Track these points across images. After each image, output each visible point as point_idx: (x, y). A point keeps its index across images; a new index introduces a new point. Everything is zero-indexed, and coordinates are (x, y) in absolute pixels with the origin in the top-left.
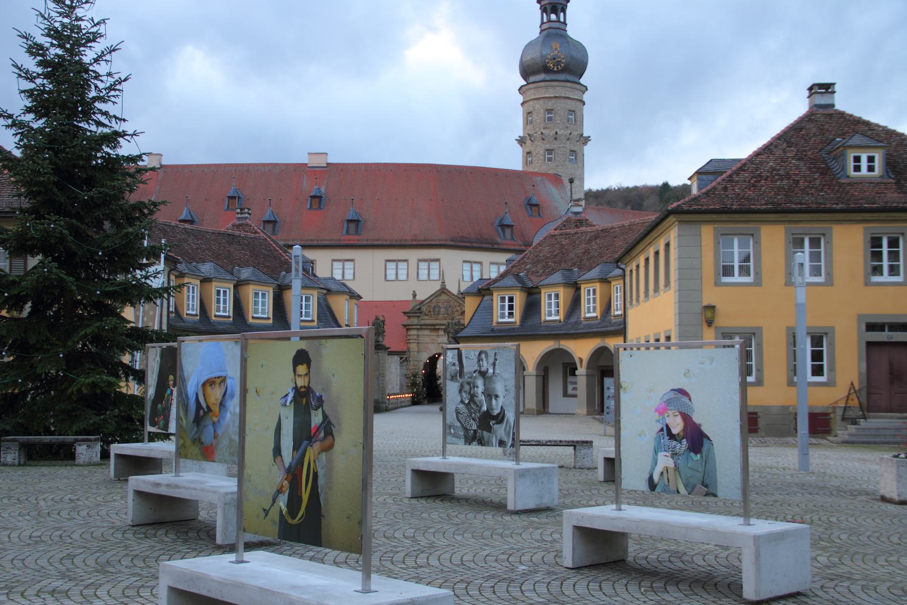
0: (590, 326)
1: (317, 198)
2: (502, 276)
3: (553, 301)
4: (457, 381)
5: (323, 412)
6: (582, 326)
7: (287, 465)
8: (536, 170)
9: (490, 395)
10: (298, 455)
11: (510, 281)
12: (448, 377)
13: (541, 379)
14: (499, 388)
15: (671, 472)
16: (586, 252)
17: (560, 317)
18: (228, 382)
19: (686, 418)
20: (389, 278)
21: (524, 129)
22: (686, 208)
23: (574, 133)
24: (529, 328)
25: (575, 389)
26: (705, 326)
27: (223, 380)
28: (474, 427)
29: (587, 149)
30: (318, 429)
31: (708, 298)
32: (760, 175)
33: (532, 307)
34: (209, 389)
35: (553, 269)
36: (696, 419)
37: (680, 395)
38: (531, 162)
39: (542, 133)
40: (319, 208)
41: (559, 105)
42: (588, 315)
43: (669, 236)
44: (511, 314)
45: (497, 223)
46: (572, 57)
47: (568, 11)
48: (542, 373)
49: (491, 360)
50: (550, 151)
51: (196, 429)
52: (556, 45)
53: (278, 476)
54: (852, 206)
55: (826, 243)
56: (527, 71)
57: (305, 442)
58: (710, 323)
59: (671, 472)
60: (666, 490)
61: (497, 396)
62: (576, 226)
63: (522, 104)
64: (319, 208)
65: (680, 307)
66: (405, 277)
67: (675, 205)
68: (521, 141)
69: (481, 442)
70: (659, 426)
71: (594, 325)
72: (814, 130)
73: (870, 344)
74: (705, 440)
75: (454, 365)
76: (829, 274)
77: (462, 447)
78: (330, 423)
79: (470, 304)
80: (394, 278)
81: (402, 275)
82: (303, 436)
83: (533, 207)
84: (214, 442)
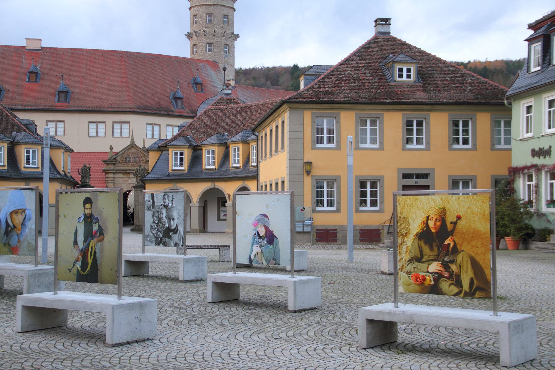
1: (34, 74)
2: (176, 138)
3: (211, 155)
4: (151, 211)
5: (99, 225)
6: (230, 173)
7: (81, 248)
8: (199, 58)
10: (86, 244)
11: (181, 141)
12: (146, 208)
13: (202, 208)
14: (175, 214)
15: (259, 254)
16: (234, 122)
17: (216, 166)
18: (27, 212)
19: (267, 228)
20: (91, 135)
21: (191, 27)
22: (294, 100)
23: (228, 32)
24: (194, 174)
27: (24, 211)
28: (161, 236)
29: (237, 44)
30: (96, 232)
31: (307, 158)
32: (341, 79)
33: (196, 159)
34: (14, 216)
35: (211, 133)
36: (271, 228)
37: (264, 217)
39: (204, 31)
40: (36, 81)
41: (217, 11)
42: (234, 165)
43: (284, 117)
44: (181, 165)
45: (171, 96)
48: (203, 205)
49: (171, 199)
50: (210, 44)
51: (6, 238)
53: (76, 254)
54: (396, 100)
55: (380, 123)
57: (90, 238)
58: (308, 173)
59: (259, 254)
61: (174, 219)
62: (227, 103)
63: (190, 8)
64: (36, 81)
65: (290, 163)
66: (103, 135)
68: (189, 36)
69: (165, 244)
70: (254, 232)
71: (238, 172)
72: (377, 49)
74: (275, 239)
75: (149, 201)
76: (381, 143)
77: (153, 247)
78: (102, 229)
79: (153, 157)
80: (95, 135)
81: (101, 133)
82: (89, 235)
83: (198, 84)
84: (18, 244)
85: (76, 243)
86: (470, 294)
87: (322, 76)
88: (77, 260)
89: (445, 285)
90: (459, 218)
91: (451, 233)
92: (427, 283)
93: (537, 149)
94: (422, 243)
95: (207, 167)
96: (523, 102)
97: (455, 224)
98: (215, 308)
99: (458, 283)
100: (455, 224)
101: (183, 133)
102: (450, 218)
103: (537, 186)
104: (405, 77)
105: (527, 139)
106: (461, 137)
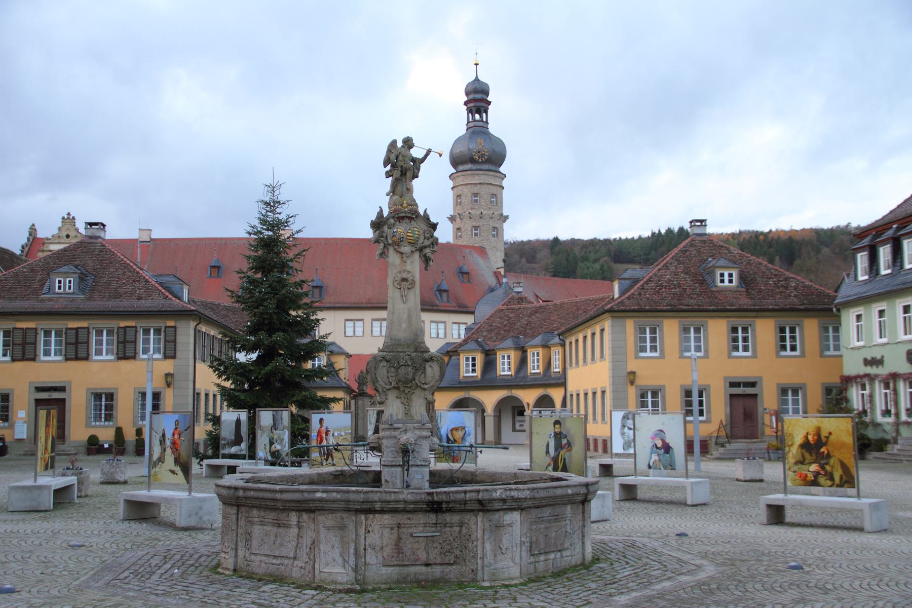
0: (536, 379)
2: (465, 341)
3: (506, 360)
8: (464, 243)
11: (472, 345)
16: (529, 323)
18: (467, 429)
19: (663, 441)
20: (347, 334)
21: (454, 209)
23: (496, 213)
24: (488, 381)
25: (521, 425)
26: (629, 385)
27: (464, 428)
31: (632, 365)
32: (661, 285)
33: (490, 364)
34: (455, 432)
36: (667, 441)
38: (461, 236)
41: (484, 190)
44: (474, 371)
45: (435, 289)
46: (494, 151)
47: (489, 112)
50: (476, 228)
52: (480, 140)
53: (548, 460)
54: (719, 307)
55: (704, 331)
56: (456, 161)
58: (632, 383)
60: (655, 468)
63: (453, 188)
66: (361, 334)
67: (609, 306)
72: (694, 252)
73: (732, 396)
76: (706, 351)
80: (352, 334)
81: (359, 332)
82: (559, 447)
83: (464, 274)
85: (547, 452)
86: (841, 485)
87: (642, 283)
88: (549, 465)
89: (822, 480)
90: (830, 433)
91: (825, 444)
92: (809, 479)
93: (869, 358)
94: (804, 451)
95: (502, 373)
96: (852, 310)
97: (827, 438)
98: (622, 503)
99: (831, 478)
100: (827, 438)
101: (472, 334)
102: (824, 434)
103: (871, 396)
104: (726, 283)
105: (859, 348)
106: (788, 343)
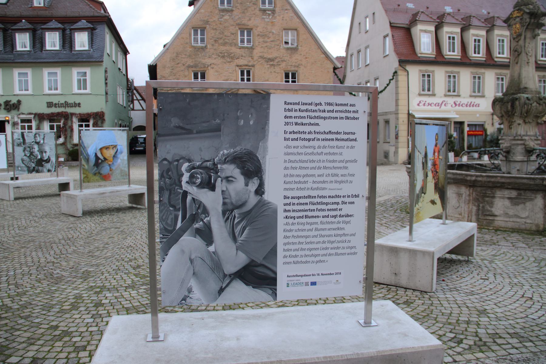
4: (21, 146)
9: (41, 152)
12: (16, 144)
14: (47, 148)
18: (119, 147)
28: (33, 165)
34: (105, 151)
49: (42, 137)
51: (96, 168)
61: (45, 152)
69: (38, 171)
75: (19, 139)
77: (26, 174)
84: (110, 172)
